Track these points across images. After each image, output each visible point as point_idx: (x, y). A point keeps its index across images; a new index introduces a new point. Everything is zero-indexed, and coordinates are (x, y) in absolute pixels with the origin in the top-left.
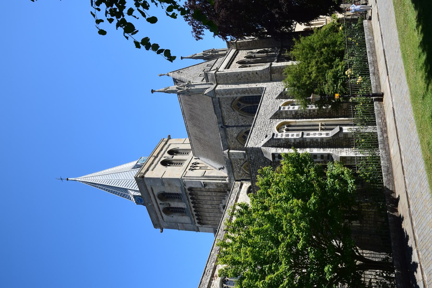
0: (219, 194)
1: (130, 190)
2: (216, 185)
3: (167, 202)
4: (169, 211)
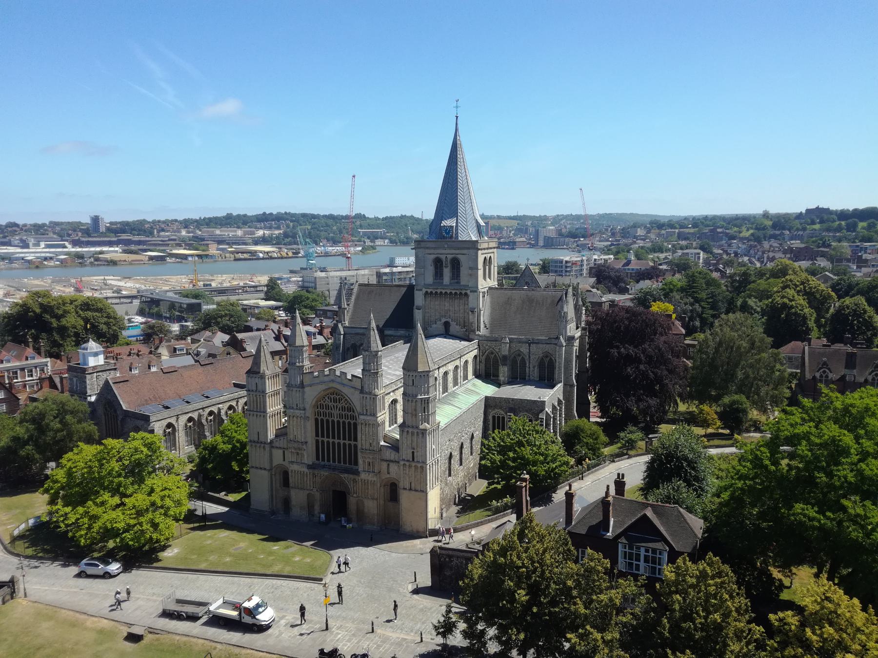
1: (457, 220)
3: (449, 265)
4: (438, 263)
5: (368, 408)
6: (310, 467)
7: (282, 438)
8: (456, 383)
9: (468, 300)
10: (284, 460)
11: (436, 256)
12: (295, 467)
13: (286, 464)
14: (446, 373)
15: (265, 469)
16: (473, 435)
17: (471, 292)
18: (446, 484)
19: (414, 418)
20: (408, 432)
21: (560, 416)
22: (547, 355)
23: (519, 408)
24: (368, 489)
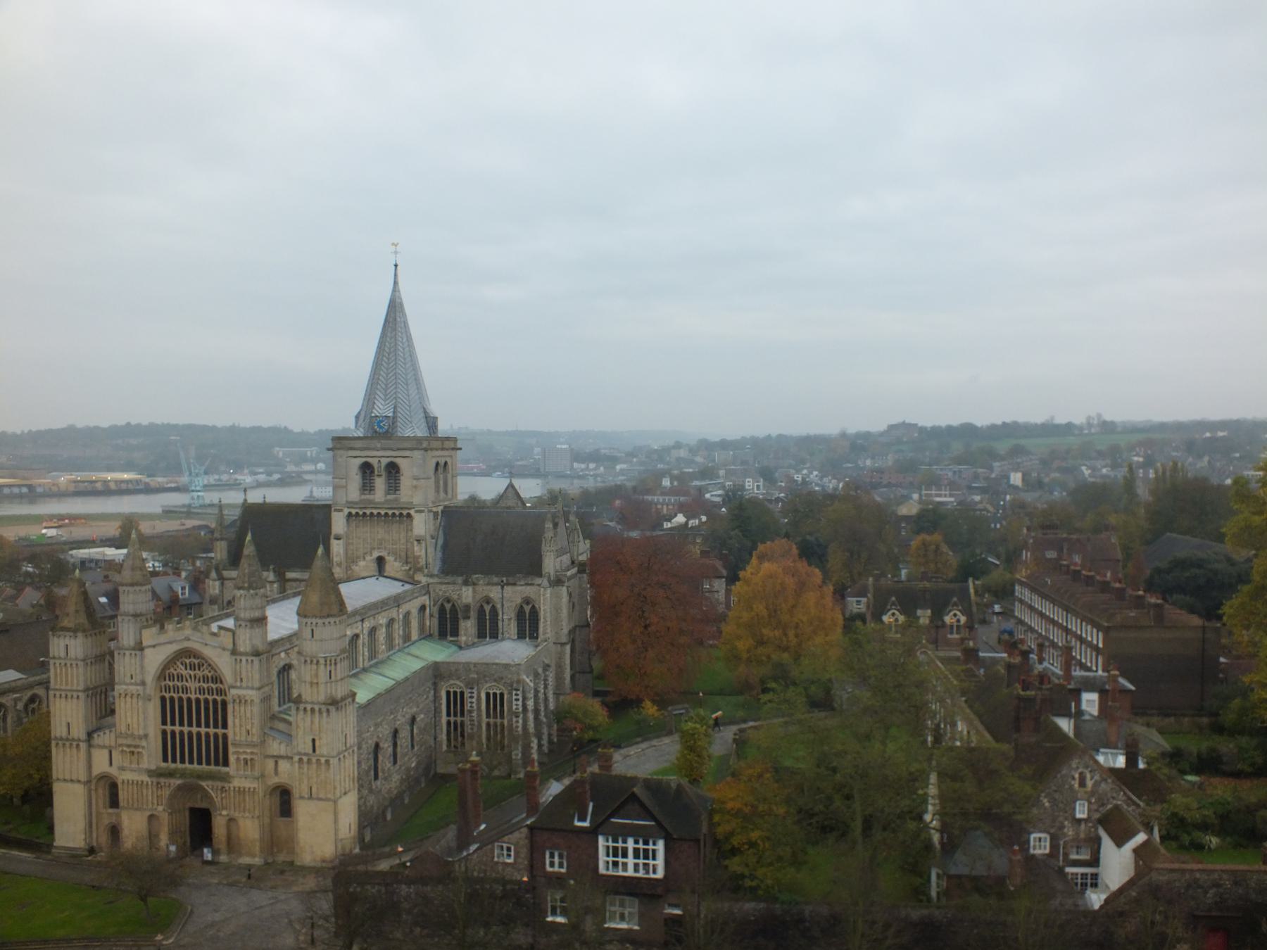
0: (403, 554)
2: (420, 556)
3: (383, 473)
4: (367, 469)
5: (244, 676)
6: (151, 773)
7: (107, 731)
8: (390, 646)
9: (411, 524)
10: (111, 764)
11: (364, 460)
12: (128, 776)
13: (113, 771)
14: (373, 631)
15: (79, 781)
16: (413, 720)
17: (417, 511)
18: (371, 791)
19: (315, 690)
20: (305, 709)
21: (546, 687)
22: (527, 601)
23: (485, 676)
24: (244, 800)
